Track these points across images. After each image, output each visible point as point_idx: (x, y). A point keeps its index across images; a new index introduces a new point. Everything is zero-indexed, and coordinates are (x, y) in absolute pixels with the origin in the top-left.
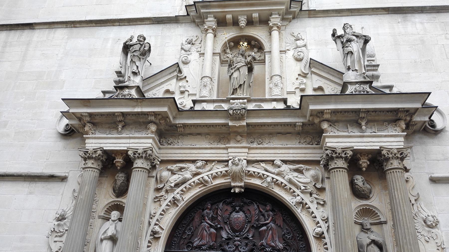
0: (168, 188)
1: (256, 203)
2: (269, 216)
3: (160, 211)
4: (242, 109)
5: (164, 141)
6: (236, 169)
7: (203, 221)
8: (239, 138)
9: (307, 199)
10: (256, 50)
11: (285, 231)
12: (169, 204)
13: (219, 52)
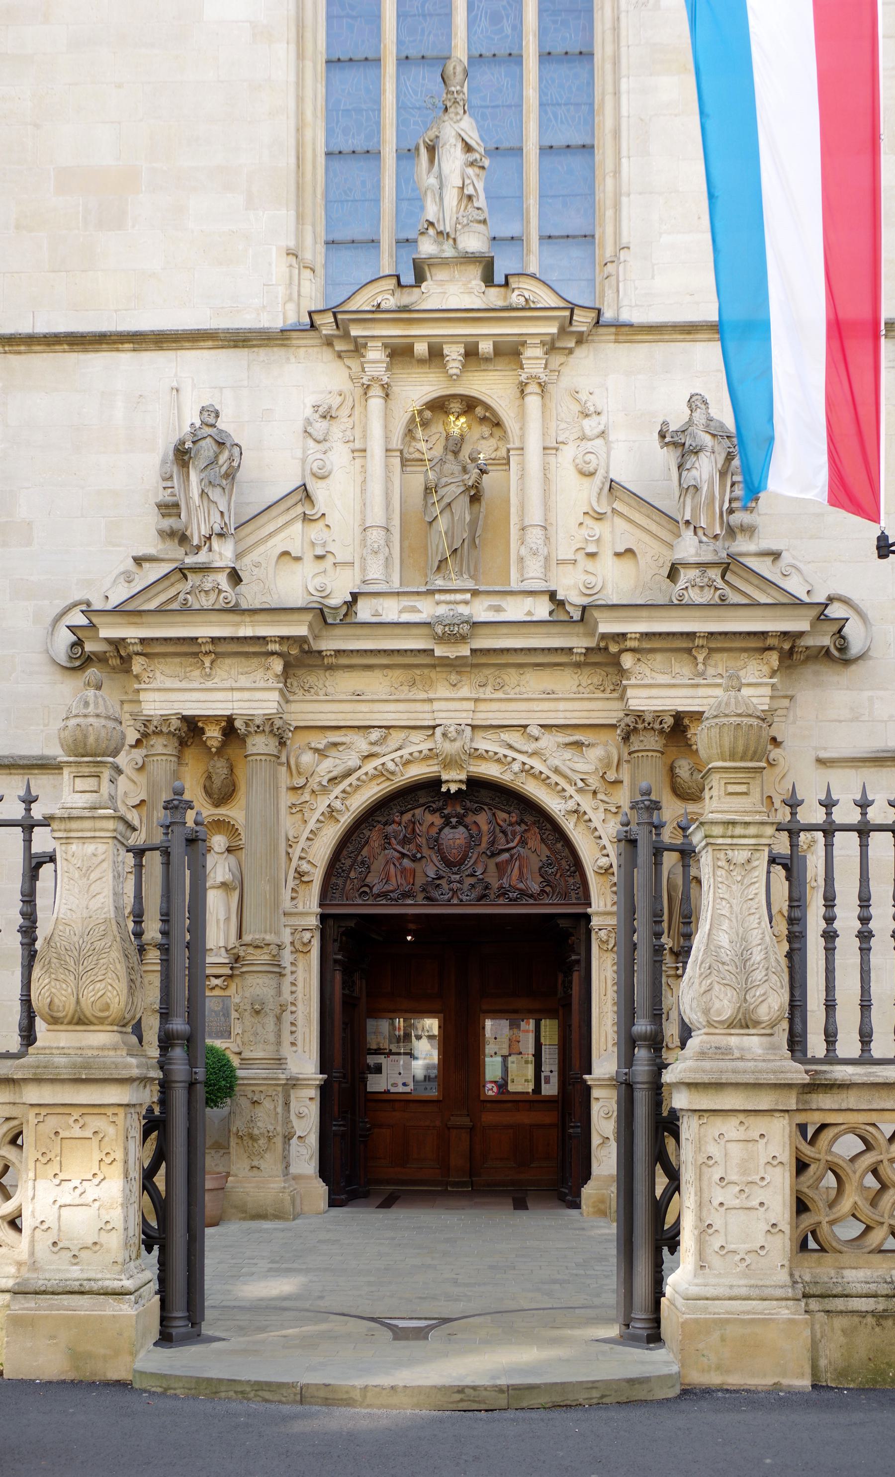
0: (315, 786)
1: (490, 809)
2: (514, 834)
3: (306, 834)
4: (463, 623)
5: (295, 684)
6: (450, 748)
7: (387, 845)
8: (454, 678)
9: (586, 803)
10: (486, 430)
11: (544, 859)
12: (322, 818)
13: (400, 447)
